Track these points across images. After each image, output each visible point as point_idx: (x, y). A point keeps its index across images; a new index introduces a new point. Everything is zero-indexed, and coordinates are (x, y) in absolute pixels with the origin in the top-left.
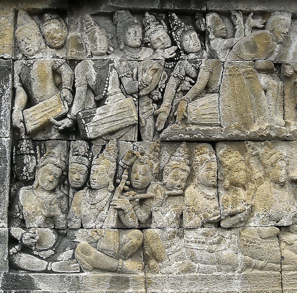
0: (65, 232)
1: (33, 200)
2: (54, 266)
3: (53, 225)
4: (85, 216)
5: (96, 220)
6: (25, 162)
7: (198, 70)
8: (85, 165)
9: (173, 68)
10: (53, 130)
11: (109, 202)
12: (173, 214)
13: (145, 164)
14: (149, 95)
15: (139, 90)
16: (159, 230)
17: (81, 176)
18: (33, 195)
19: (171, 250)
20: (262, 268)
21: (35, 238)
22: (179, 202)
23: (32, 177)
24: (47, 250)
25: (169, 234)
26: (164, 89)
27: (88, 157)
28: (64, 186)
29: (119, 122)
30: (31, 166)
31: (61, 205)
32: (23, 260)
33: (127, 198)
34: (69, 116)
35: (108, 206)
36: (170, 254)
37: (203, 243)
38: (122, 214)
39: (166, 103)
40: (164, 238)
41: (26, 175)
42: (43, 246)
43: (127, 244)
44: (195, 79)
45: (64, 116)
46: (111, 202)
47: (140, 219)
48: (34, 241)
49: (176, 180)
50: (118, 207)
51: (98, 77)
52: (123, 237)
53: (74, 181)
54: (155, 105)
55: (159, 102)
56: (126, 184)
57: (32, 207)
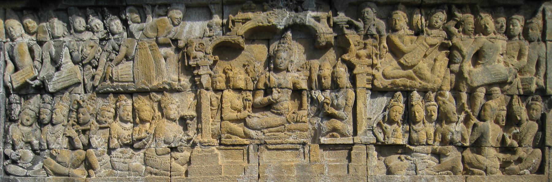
2: (30, 173)
6: (13, 108)
7: (119, 46)
9: (105, 44)
10: (30, 88)
14: (90, 63)
15: (82, 60)
20: (156, 174)
26: (99, 59)
27: (51, 104)
29: (69, 81)
32: (12, 168)
34: (38, 78)
37: (120, 158)
39: (100, 68)
41: (15, 116)
44: (118, 52)
45: (35, 78)
48: (18, 157)
51: (56, 52)
54: (94, 70)
55: (96, 67)
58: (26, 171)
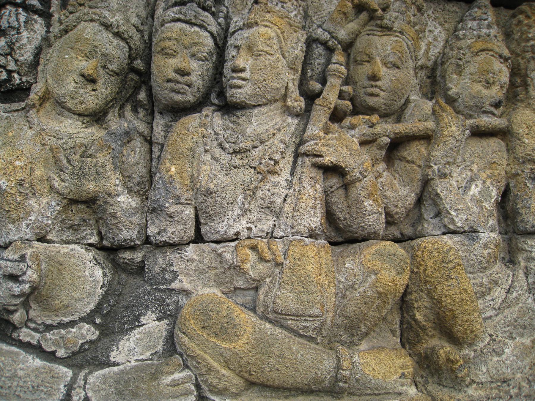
0: (138, 256)
1: (23, 142)
3: (95, 232)
4: (209, 192)
5: (252, 206)
8: (206, 29)
11: (292, 147)
12: (491, 188)
13: (398, 34)
16: (457, 238)
17: (194, 65)
18: (25, 128)
19: (491, 303)
21: (20, 279)
22: (499, 153)
23: (28, 79)
24: (72, 324)
25: (486, 252)
28: (135, 110)
30: (25, 41)
31: (123, 162)
33: (353, 132)
35: (289, 158)
36: (490, 317)
38: (337, 189)
40: (473, 266)
42: (56, 311)
43: (361, 290)
46: (302, 142)
47: (392, 208)
49: (488, 85)
50: (327, 160)
52: (347, 266)
53: (169, 81)
56: (341, 96)
57: (18, 163)
58: (66, 372)
